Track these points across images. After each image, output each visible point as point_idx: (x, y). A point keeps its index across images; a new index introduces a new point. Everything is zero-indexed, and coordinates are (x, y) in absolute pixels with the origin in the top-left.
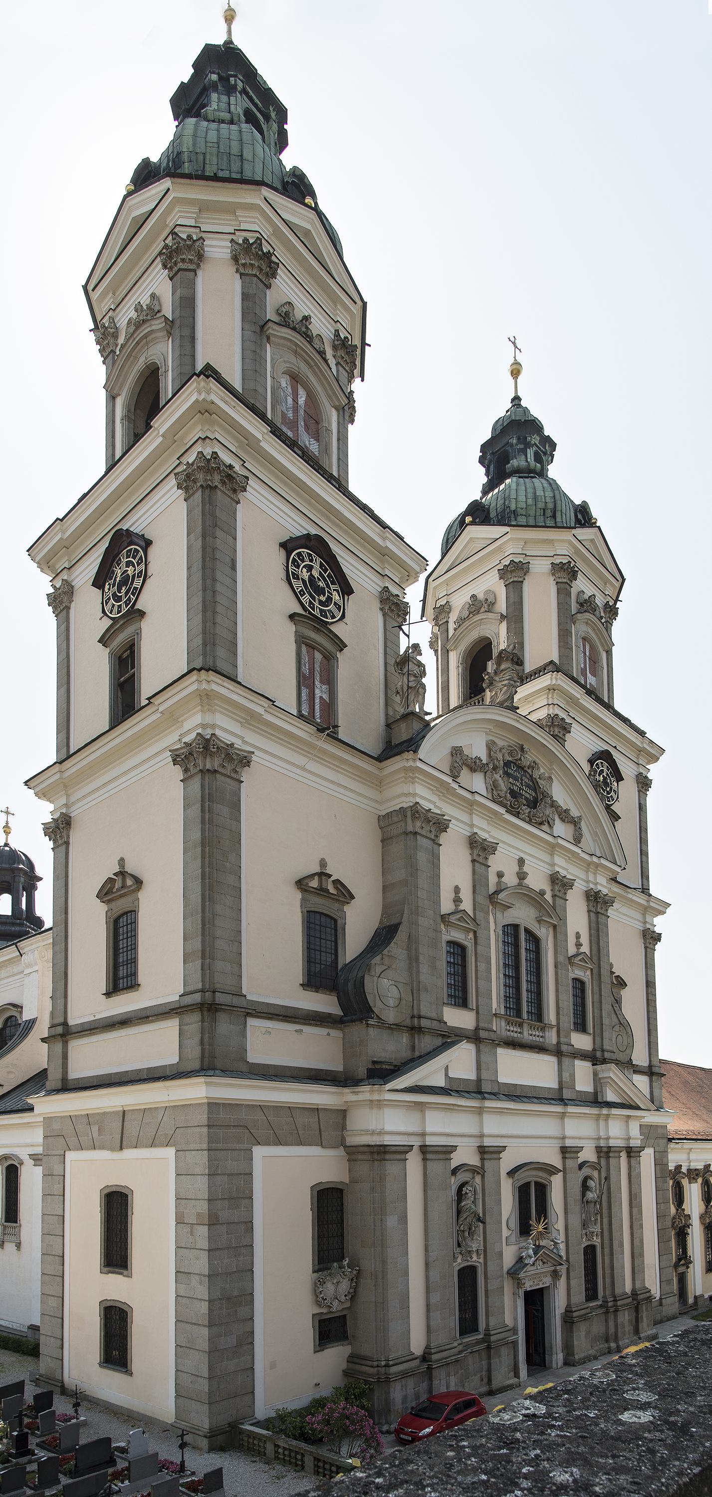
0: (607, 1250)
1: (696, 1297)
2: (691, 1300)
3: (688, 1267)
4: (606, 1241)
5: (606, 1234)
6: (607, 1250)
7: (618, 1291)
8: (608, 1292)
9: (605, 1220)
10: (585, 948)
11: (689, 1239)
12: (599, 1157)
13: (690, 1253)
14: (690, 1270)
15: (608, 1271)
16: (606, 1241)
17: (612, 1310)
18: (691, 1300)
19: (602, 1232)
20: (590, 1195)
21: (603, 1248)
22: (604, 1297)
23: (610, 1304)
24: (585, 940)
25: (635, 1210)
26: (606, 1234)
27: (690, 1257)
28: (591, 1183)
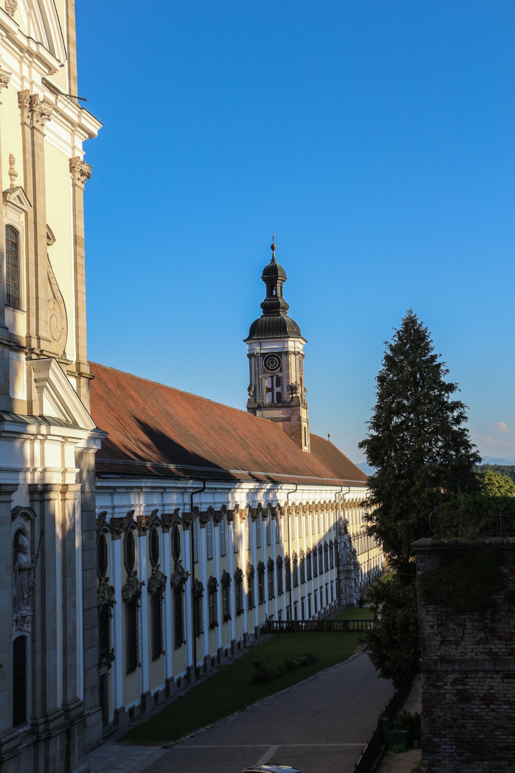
0: (38, 644)
1: (117, 713)
2: (111, 718)
3: (109, 667)
4: (38, 630)
5: (38, 619)
6: (38, 644)
7: (50, 707)
8: (38, 710)
9: (38, 597)
10: (19, 182)
11: (112, 622)
12: (32, 501)
13: (112, 645)
14: (112, 671)
15: (39, 677)
16: (38, 630)
17: (44, 736)
18: (111, 718)
19: (33, 617)
20: (25, 559)
21: (33, 641)
22: (34, 718)
23: (41, 728)
24: (19, 168)
25: (69, 580)
26: (38, 619)
27: (113, 650)
28: (25, 541)
